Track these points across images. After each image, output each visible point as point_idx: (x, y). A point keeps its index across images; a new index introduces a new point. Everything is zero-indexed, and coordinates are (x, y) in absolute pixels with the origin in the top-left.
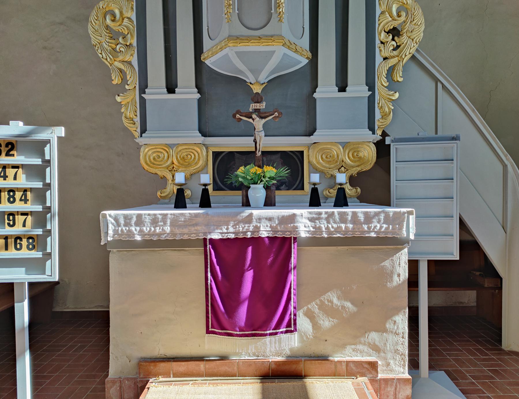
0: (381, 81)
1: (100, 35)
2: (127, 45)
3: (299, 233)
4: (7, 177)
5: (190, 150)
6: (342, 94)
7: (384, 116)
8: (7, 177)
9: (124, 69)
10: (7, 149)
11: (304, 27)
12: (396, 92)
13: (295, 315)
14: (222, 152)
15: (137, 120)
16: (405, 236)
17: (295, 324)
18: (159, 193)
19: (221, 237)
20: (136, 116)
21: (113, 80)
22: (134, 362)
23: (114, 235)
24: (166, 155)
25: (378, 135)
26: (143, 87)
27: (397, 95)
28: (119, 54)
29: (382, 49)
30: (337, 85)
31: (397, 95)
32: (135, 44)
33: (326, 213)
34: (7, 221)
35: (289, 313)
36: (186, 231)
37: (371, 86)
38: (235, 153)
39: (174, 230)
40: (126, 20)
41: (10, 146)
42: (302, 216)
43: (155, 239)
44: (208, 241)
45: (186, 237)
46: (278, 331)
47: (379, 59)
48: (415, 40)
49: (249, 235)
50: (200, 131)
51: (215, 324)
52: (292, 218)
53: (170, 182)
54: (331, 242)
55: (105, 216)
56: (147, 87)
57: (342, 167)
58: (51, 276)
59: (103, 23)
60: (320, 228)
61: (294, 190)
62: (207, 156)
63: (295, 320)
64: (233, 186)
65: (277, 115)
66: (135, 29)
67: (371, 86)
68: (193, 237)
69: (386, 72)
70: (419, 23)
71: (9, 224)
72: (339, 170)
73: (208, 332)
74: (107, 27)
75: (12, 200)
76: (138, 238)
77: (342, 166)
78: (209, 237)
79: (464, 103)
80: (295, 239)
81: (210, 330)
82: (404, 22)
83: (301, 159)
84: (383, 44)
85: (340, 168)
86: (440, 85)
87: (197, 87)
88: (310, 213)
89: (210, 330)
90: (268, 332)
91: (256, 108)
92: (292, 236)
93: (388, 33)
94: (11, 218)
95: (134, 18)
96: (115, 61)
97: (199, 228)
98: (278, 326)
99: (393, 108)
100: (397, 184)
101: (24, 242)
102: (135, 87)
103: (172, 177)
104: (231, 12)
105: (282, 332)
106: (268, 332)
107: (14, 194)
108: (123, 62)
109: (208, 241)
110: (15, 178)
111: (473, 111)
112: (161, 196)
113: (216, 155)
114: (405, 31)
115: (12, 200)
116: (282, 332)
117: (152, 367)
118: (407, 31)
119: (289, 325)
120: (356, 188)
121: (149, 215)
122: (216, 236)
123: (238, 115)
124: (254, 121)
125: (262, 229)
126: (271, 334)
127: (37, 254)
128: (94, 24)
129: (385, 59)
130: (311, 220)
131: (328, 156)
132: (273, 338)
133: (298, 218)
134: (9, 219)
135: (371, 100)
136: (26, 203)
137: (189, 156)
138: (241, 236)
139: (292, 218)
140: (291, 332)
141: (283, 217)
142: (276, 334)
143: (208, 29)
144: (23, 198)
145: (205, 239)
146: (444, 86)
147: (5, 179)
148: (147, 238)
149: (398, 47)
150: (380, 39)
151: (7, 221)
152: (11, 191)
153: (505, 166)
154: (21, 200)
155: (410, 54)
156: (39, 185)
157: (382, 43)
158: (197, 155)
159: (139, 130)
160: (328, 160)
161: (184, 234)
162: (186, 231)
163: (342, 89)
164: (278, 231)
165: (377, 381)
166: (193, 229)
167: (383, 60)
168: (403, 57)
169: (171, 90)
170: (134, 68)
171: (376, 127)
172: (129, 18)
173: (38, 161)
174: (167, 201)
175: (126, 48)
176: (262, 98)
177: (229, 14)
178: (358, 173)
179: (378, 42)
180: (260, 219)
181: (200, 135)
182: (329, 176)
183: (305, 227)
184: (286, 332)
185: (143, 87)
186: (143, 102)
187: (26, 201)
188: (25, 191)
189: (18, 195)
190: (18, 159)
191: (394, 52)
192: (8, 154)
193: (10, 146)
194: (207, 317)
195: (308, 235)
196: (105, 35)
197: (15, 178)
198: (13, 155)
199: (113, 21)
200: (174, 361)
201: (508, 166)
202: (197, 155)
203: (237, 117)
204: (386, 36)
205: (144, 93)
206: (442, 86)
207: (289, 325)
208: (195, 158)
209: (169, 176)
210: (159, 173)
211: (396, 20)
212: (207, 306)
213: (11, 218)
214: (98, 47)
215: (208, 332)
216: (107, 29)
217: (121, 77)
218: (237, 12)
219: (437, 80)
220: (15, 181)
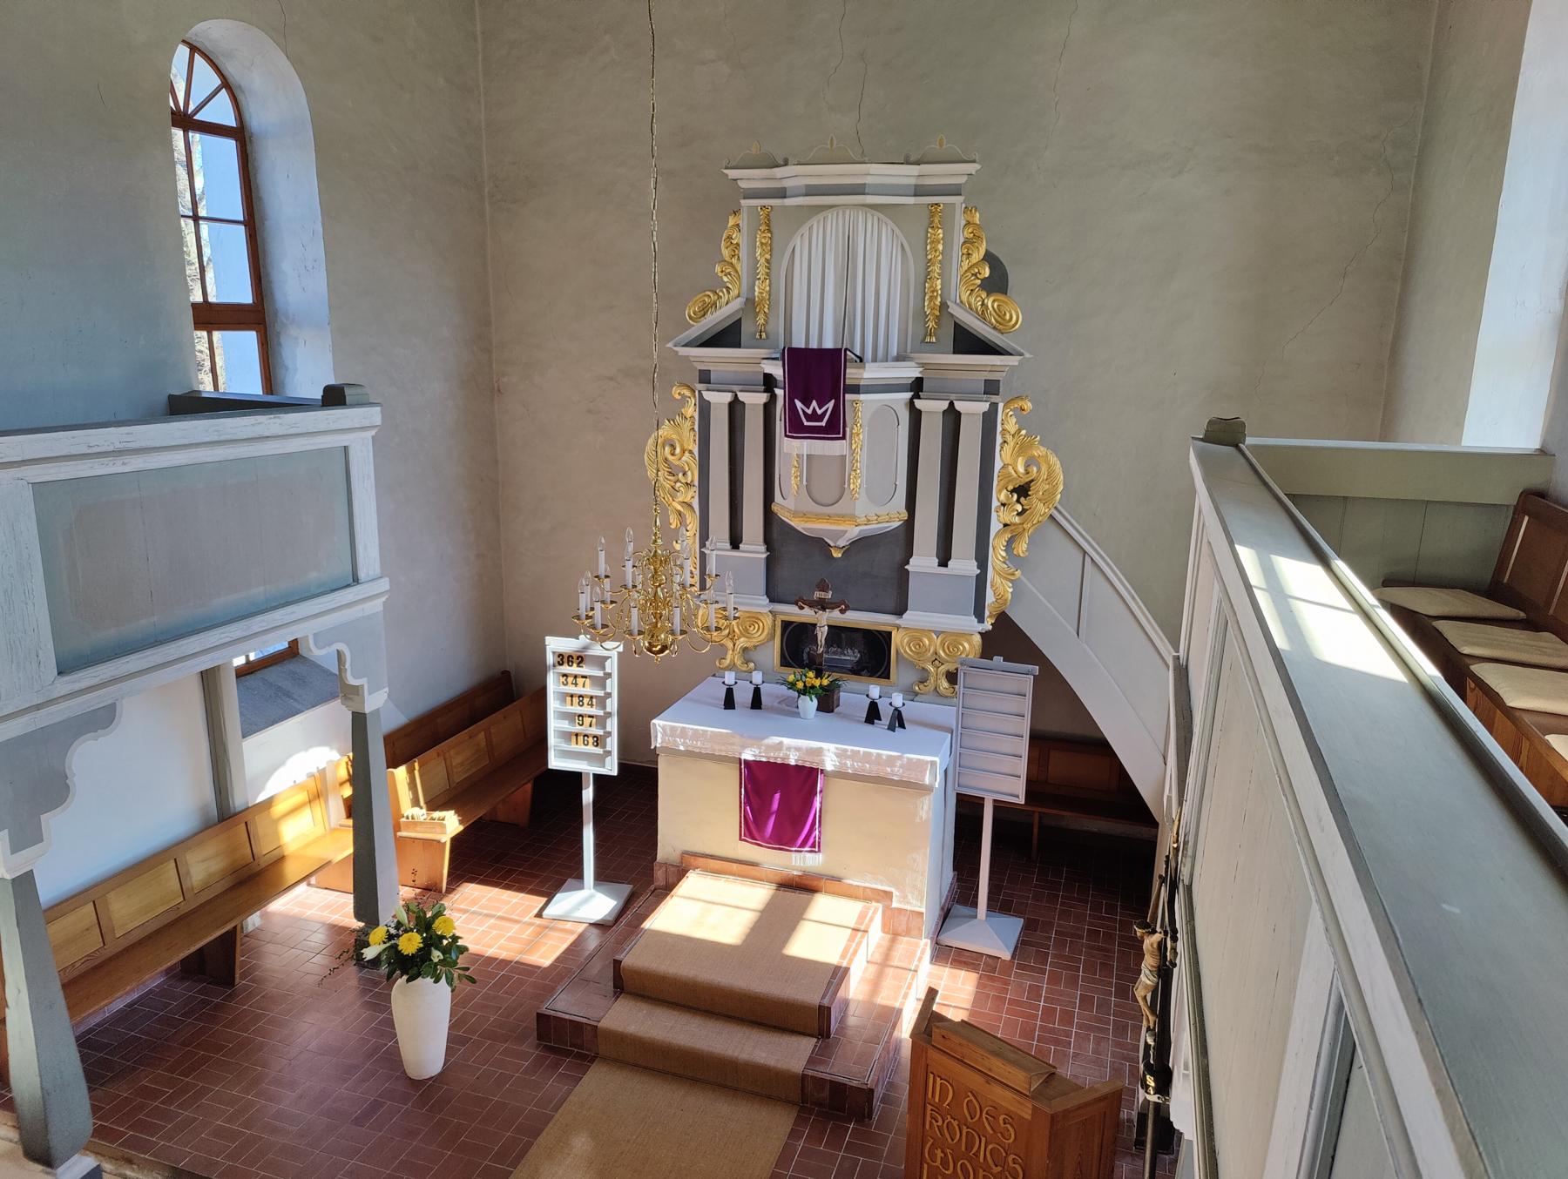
13: (819, 838)
14: (793, 622)
17: (819, 847)
33: (852, 750)
35: (813, 836)
43: (697, 751)
45: (724, 754)
50: (768, 594)
51: (747, 834)
52: (819, 751)
53: (730, 652)
54: (856, 777)
55: (655, 724)
60: (846, 764)
62: (774, 625)
63: (819, 843)
73: (741, 839)
76: (682, 748)
80: (822, 770)
88: (837, 749)
90: (794, 849)
97: (735, 747)
98: (803, 845)
103: (732, 646)
105: (806, 851)
106: (794, 849)
113: (786, 625)
116: (806, 851)
121: (692, 729)
126: (796, 851)
130: (837, 755)
132: (798, 854)
137: (753, 627)
139: (819, 751)
140: (815, 852)
141: (811, 749)
142: (801, 851)
145: (740, 759)
148: (690, 749)
158: (761, 625)
173: (601, 674)
181: (768, 600)
194: (741, 827)
195: (833, 768)
202: (761, 625)
205: (705, 546)
207: (813, 846)
208: (759, 628)
209: (730, 645)
212: (741, 817)
215: (741, 839)
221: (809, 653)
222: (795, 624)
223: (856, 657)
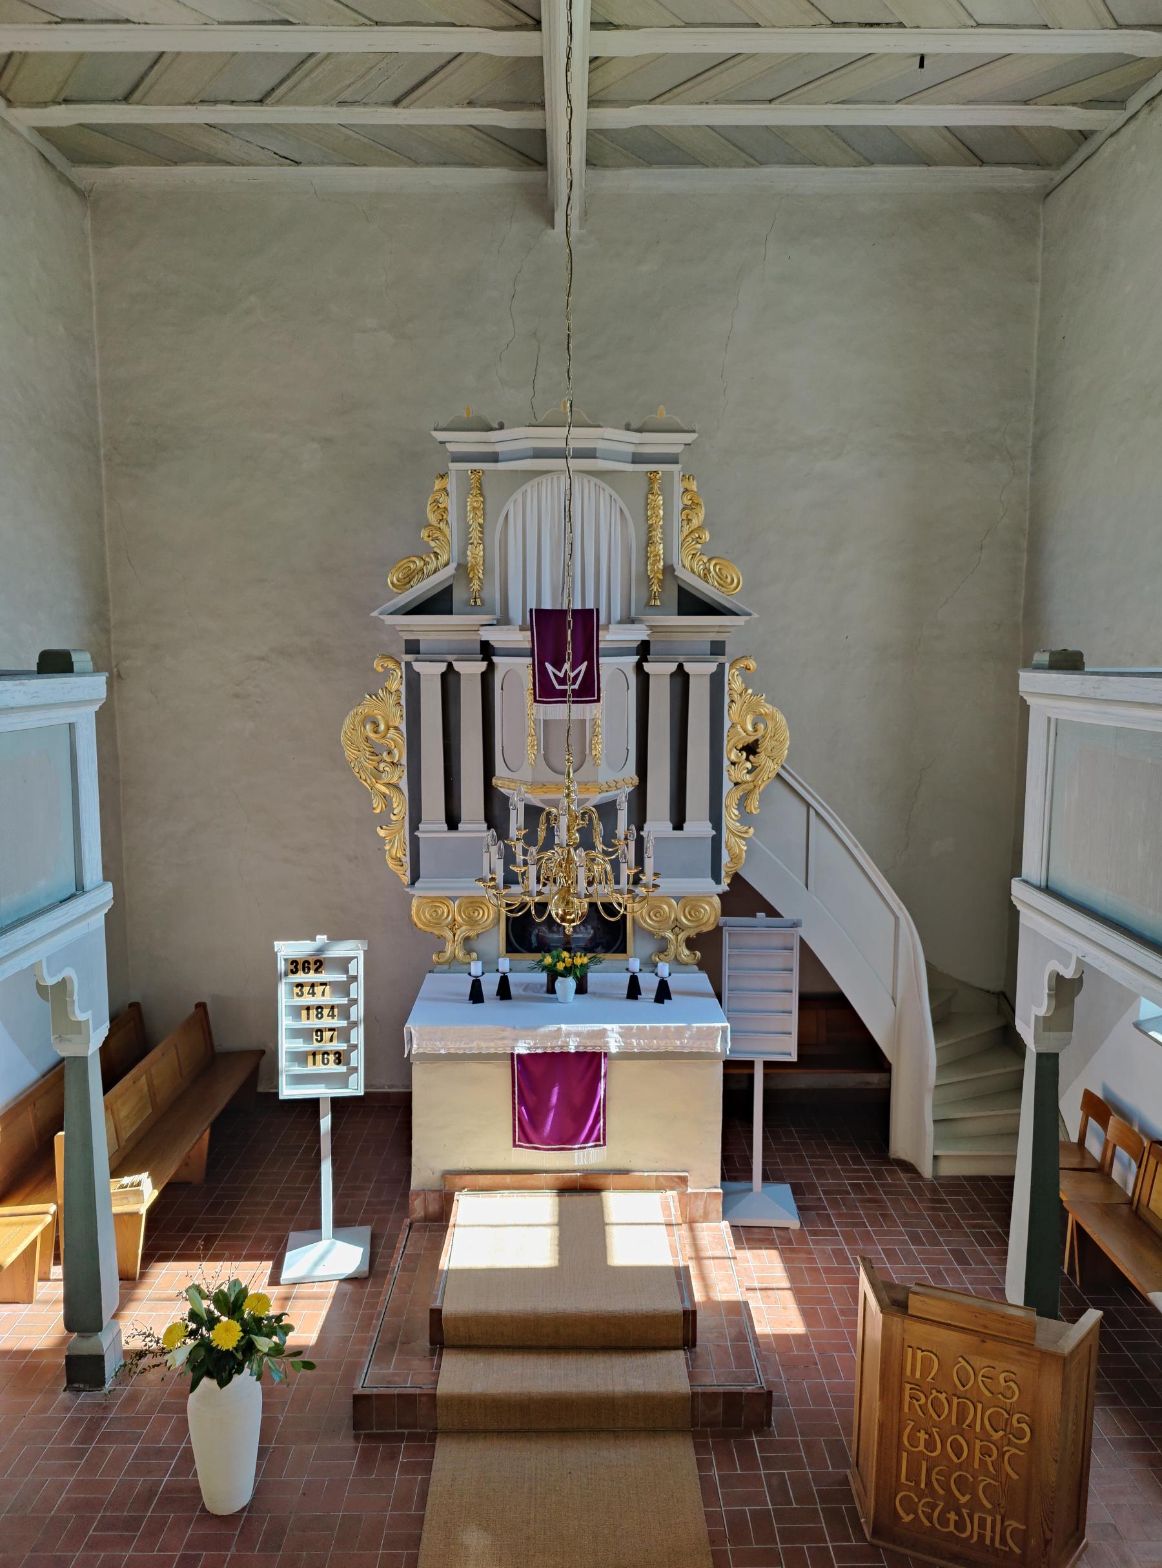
0: (730, 814)
2: (393, 763)
3: (610, 1049)
4: (315, 994)
5: (478, 904)
6: (678, 833)
7: (734, 858)
8: (315, 994)
9: (389, 793)
10: (316, 966)
11: (629, 748)
12: (750, 828)
15: (407, 860)
16: (719, 1051)
18: (434, 957)
19: (528, 1052)
20: (405, 855)
21: (374, 809)
22: (438, 1175)
23: (418, 1048)
24: (446, 910)
25: (726, 884)
26: (415, 818)
27: (752, 830)
28: (384, 774)
29: (732, 772)
30: (671, 821)
31: (752, 830)
32: (404, 761)
34: (315, 1037)
36: (492, 1044)
37: (716, 819)
39: (480, 1044)
40: (392, 731)
41: (318, 964)
42: (613, 1031)
44: (515, 1057)
45: (492, 1051)
46: (586, 1145)
47: (727, 785)
48: (775, 761)
49: (557, 1050)
51: (522, 1137)
52: (603, 1034)
57: (677, 926)
58: (358, 1089)
60: (631, 1043)
61: (614, 953)
64: (533, 946)
66: (405, 743)
67: (716, 819)
68: (500, 1051)
69: (737, 802)
70: (782, 739)
71: (317, 1040)
73: (515, 1145)
74: (367, 739)
75: (320, 1016)
77: (676, 926)
78: (516, 1052)
80: (605, 1054)
81: (517, 1143)
82: (763, 737)
84: (733, 767)
85: (674, 928)
86: (812, 812)
88: (621, 1028)
89: (517, 1143)
92: (603, 1051)
93: (740, 751)
94: (319, 1034)
95: (403, 728)
96: (377, 782)
97: (506, 1042)
98: (586, 1140)
99: (745, 848)
100: (730, 974)
101: (332, 1057)
102: (403, 817)
104: (535, 753)
106: (576, 1146)
107: (322, 1011)
108: (388, 785)
109: (515, 1057)
110: (323, 994)
112: (437, 962)
114: (764, 747)
115: (320, 1016)
117: (457, 1180)
118: (766, 748)
119: (598, 1139)
120: (694, 954)
122: (522, 1049)
125: (571, 1043)
127: (342, 1069)
128: (349, 734)
129: (736, 784)
131: (658, 915)
133: (610, 1034)
134: (317, 1035)
135: (716, 842)
136: (333, 1018)
138: (549, 1051)
142: (585, 1148)
143: (503, 750)
144: (330, 1014)
145: (512, 1054)
147: (313, 996)
149: (754, 768)
150: (729, 759)
151: (315, 1037)
152: (319, 1008)
154: (328, 1016)
155: (769, 778)
156: (345, 1001)
157: (733, 764)
159: (408, 873)
160: (658, 919)
161: (491, 1048)
162: (492, 1044)
163: (678, 825)
164: (588, 1046)
165: (687, 1194)
166: (499, 1043)
167: (733, 785)
168: (760, 783)
169: (453, 821)
170: (403, 794)
171: (723, 874)
172: (396, 728)
173: (343, 978)
174: (446, 967)
177: (533, 755)
178: (698, 935)
179: (726, 763)
180: (568, 1035)
182: (659, 938)
183: (616, 1041)
184: (596, 1146)
185: (415, 818)
186: (415, 842)
187: (333, 1016)
188: (333, 1007)
189: (326, 1012)
190: (323, 976)
191: (748, 776)
192: (316, 971)
193: (318, 964)
194: (514, 1131)
196: (365, 749)
197: (323, 994)
198: (322, 972)
199: (376, 732)
200: (479, 1174)
204: (738, 755)
207: (598, 1139)
210: (436, 932)
211: (750, 736)
212: (514, 1120)
213: (319, 1034)
214: (355, 765)
215: (515, 1145)
216: (367, 742)
217: (385, 803)
218: (542, 752)
220: (323, 998)
221: (537, 936)
223: (589, 933)
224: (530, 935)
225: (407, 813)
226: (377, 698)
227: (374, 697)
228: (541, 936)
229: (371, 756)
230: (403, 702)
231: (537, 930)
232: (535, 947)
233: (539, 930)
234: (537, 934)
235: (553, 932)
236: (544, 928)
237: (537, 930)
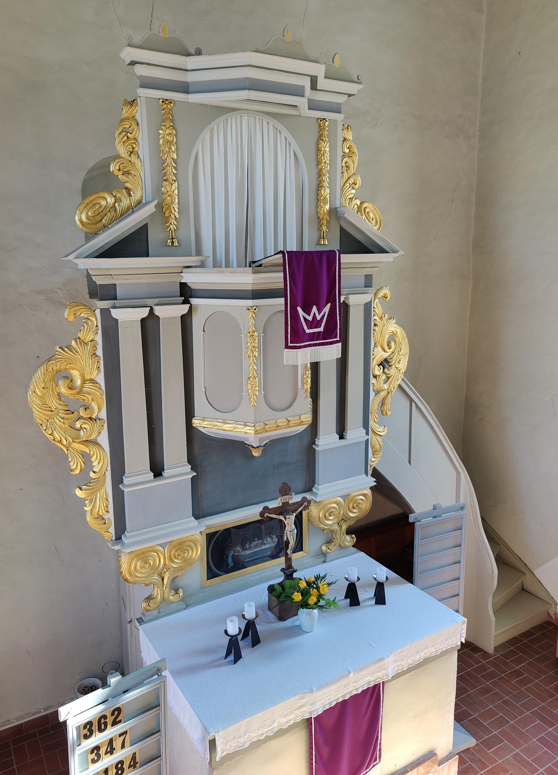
1: (49, 409)
2: (90, 418)
14: (217, 532)
32: (103, 415)
38: (232, 529)
56: (123, 472)
59: (54, 391)
65: (307, 504)
66: (104, 396)
72: (338, 524)
79: (432, 420)
83: (300, 519)
87: (189, 462)
91: (285, 501)
111: (438, 426)
123: (267, 514)
124: (286, 520)
146: (417, 406)
153: (458, 473)
170: (103, 449)
172: (93, 381)
175: (92, 424)
176: (290, 488)
201: (461, 473)
203: (265, 516)
206: (416, 406)
219: (411, 401)
221: (233, 556)
222: (219, 533)
223: (274, 542)
224: (227, 558)
225: (109, 468)
226: (71, 351)
227: (66, 349)
228: (237, 556)
229: (67, 414)
230: (100, 352)
231: (232, 552)
232: (232, 567)
233: (234, 552)
234: (233, 555)
235: (246, 549)
236: (238, 548)
237: (232, 552)
